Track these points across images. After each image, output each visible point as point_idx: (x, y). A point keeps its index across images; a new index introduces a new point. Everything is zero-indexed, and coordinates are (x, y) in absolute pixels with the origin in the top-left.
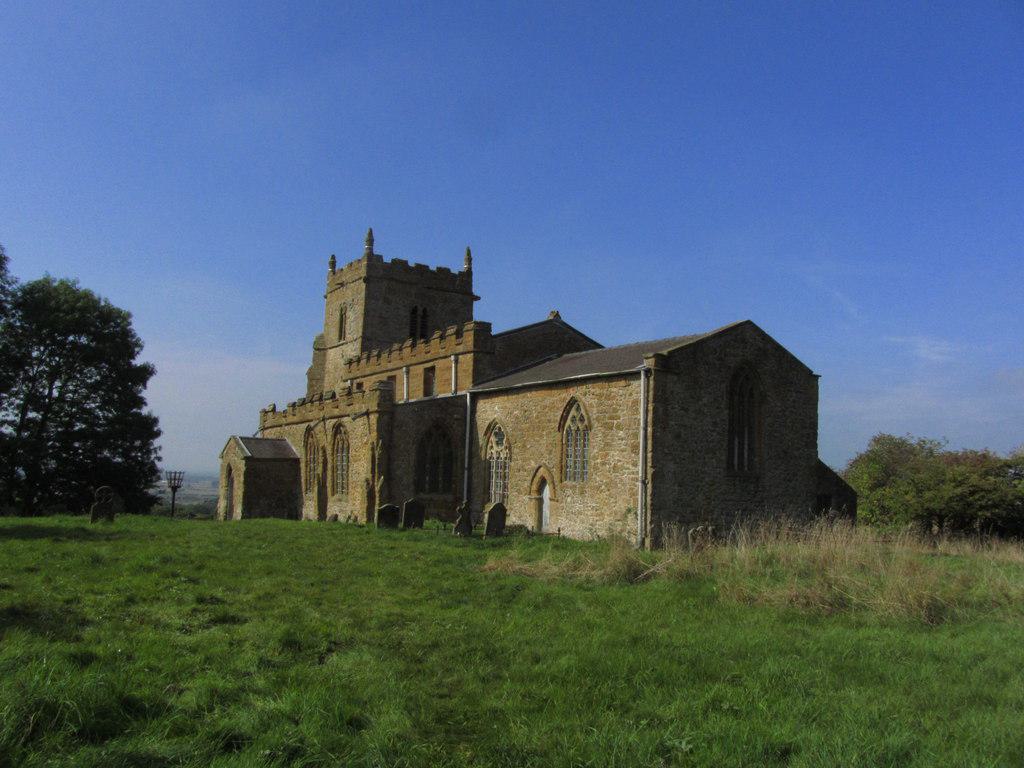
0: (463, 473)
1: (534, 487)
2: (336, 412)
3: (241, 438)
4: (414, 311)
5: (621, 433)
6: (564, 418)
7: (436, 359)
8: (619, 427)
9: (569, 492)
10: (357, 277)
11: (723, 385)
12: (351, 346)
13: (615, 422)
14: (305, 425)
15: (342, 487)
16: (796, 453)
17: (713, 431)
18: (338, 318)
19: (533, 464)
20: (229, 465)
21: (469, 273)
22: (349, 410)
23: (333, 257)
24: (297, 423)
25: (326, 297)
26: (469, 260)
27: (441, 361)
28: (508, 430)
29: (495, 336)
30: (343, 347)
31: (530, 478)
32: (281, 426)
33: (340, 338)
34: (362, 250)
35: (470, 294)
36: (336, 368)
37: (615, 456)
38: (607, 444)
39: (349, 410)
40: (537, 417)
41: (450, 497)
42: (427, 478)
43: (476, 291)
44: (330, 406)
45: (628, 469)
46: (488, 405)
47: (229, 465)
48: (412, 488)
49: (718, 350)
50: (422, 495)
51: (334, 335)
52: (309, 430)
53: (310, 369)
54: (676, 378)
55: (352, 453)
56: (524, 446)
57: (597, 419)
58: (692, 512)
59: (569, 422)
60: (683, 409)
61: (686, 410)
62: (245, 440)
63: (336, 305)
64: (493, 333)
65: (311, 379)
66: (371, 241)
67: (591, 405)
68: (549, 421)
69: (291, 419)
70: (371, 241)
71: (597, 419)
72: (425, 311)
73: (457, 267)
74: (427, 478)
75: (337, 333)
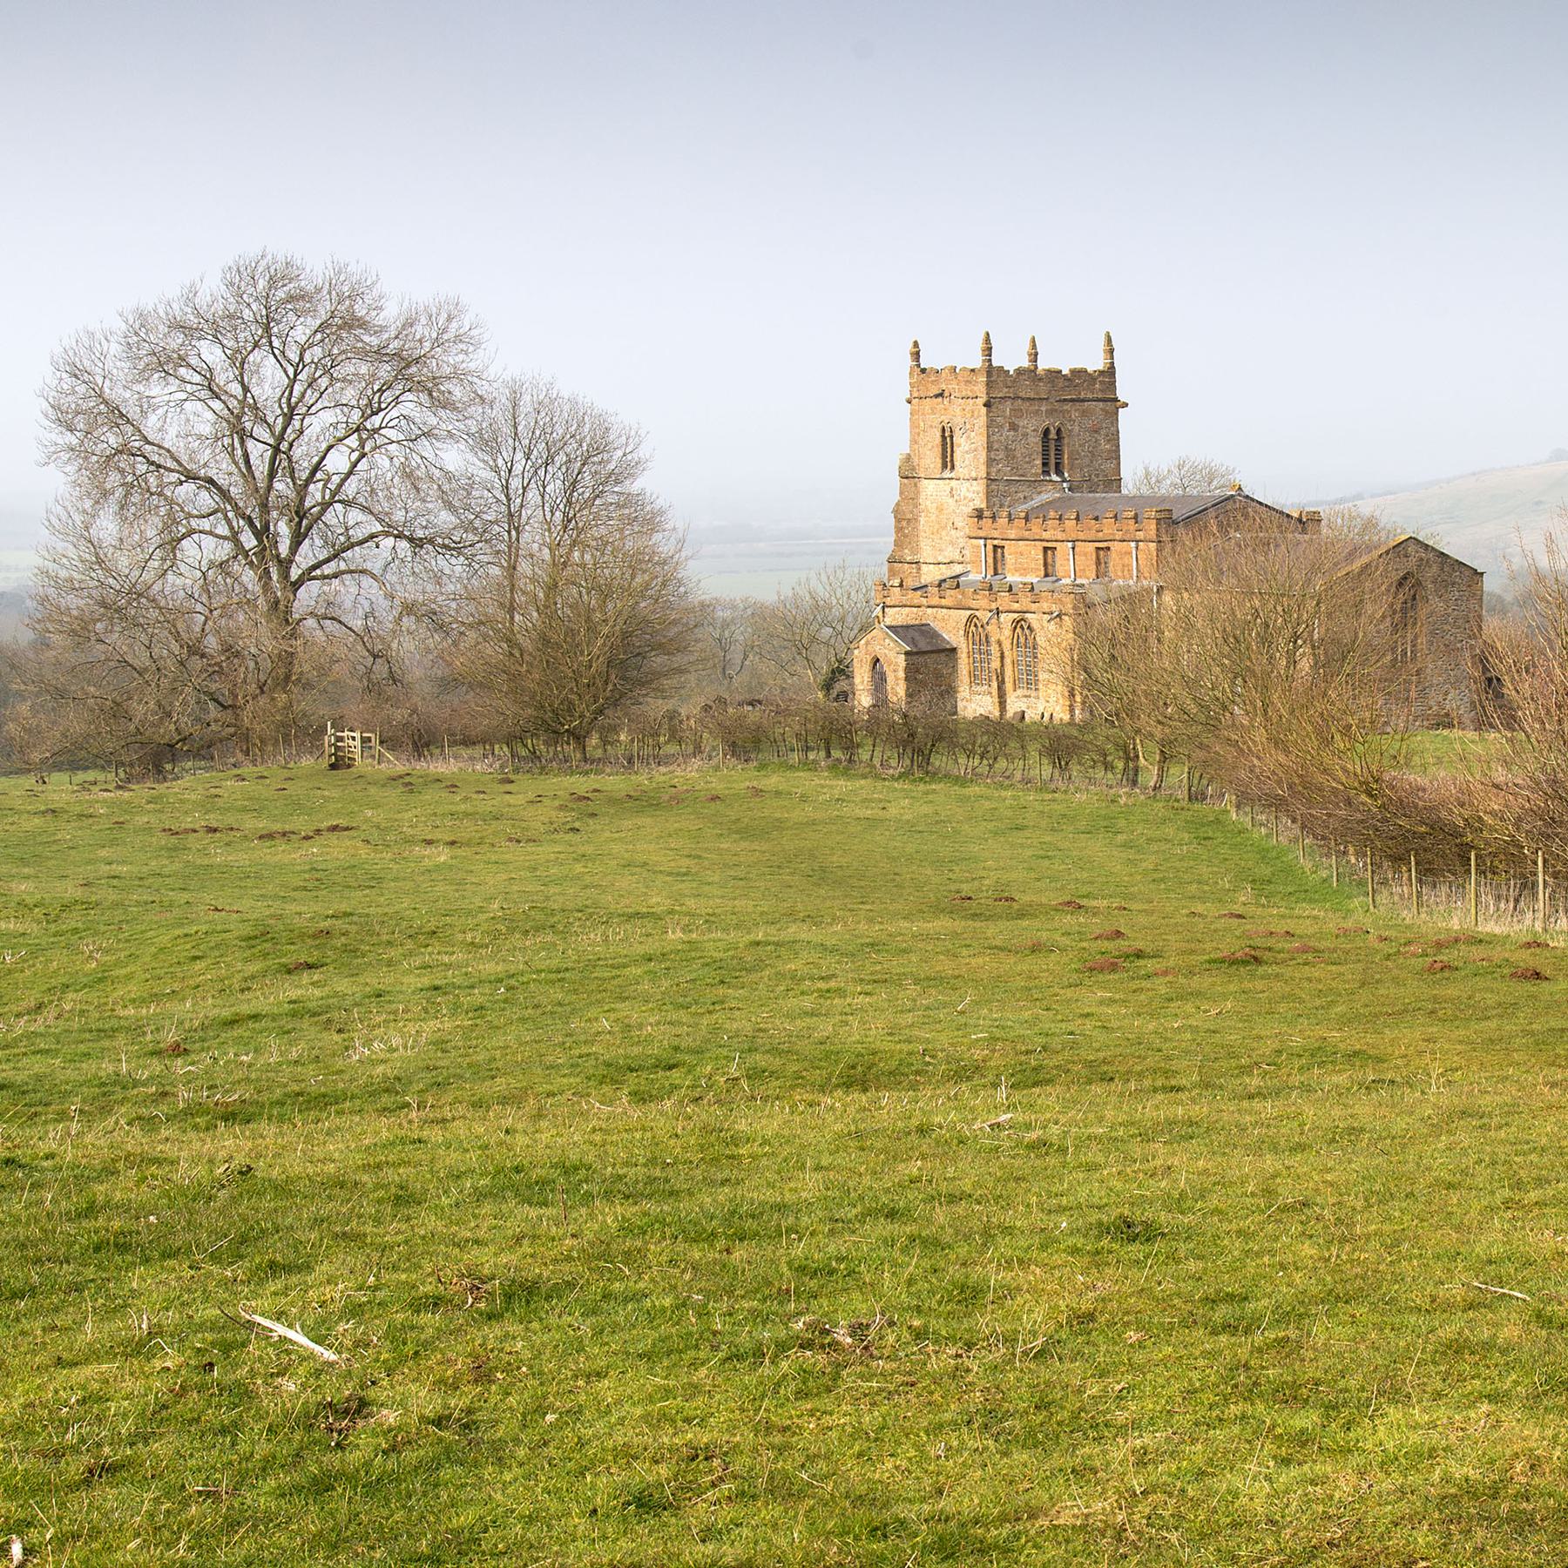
4: (1046, 432)
14: (969, 613)
18: (938, 439)
21: (1110, 372)
26: (1111, 351)
30: (953, 483)
33: (944, 466)
34: (977, 362)
35: (1116, 400)
43: (1121, 394)
51: (930, 459)
53: (898, 504)
65: (898, 520)
66: (988, 351)
70: (988, 351)
72: (1059, 431)
75: (939, 461)
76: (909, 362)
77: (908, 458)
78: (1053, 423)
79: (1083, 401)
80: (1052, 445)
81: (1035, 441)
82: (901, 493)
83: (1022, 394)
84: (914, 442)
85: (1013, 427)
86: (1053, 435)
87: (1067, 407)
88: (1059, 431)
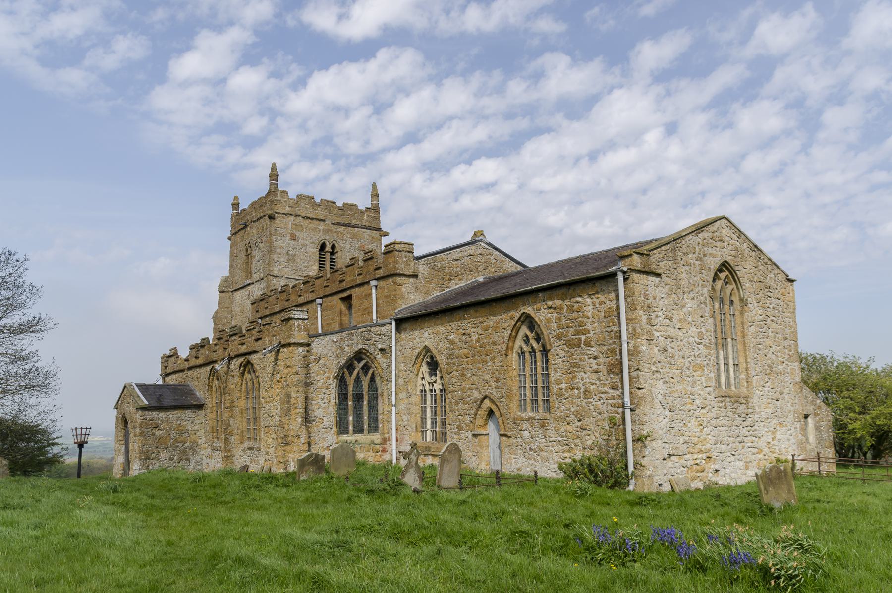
0: (390, 411)
1: (480, 421)
2: (243, 349)
3: (137, 385)
4: (323, 247)
5: (593, 351)
6: (513, 338)
7: (352, 287)
8: (588, 344)
9: (525, 425)
10: (262, 214)
11: (705, 290)
12: (257, 286)
13: (583, 337)
15: (253, 431)
16: (781, 367)
17: (700, 344)
19: (476, 395)
20: (124, 416)
21: (375, 209)
22: (257, 346)
23: (236, 198)
24: (200, 366)
25: (229, 239)
26: (375, 195)
27: (357, 289)
28: (441, 359)
29: (419, 258)
31: (472, 412)
32: (182, 371)
35: (379, 230)
36: (243, 311)
37: (585, 378)
38: (575, 365)
39: (257, 346)
40: (478, 340)
41: (376, 438)
42: (351, 418)
43: (384, 228)
44: (236, 343)
45: (605, 393)
46: (416, 333)
47: (124, 416)
48: (335, 428)
49: (697, 249)
50: (345, 437)
52: (213, 372)
53: (216, 312)
54: (657, 280)
55: (263, 393)
56: (463, 375)
57: (559, 337)
58: (686, 442)
59: (520, 342)
60: (667, 317)
61: (670, 319)
62: (143, 388)
63: (242, 246)
64: (417, 254)
67: (549, 321)
68: (494, 343)
69: (193, 362)
71: (559, 337)
72: (333, 247)
73: (363, 202)
74: (351, 418)
76: (230, 211)
77: (227, 279)
78: (329, 240)
79: (354, 227)
80: (328, 256)
81: (314, 251)
82: (219, 303)
83: (303, 214)
84: (231, 266)
85: (293, 238)
86: (328, 248)
87: (341, 229)
88: (333, 247)
